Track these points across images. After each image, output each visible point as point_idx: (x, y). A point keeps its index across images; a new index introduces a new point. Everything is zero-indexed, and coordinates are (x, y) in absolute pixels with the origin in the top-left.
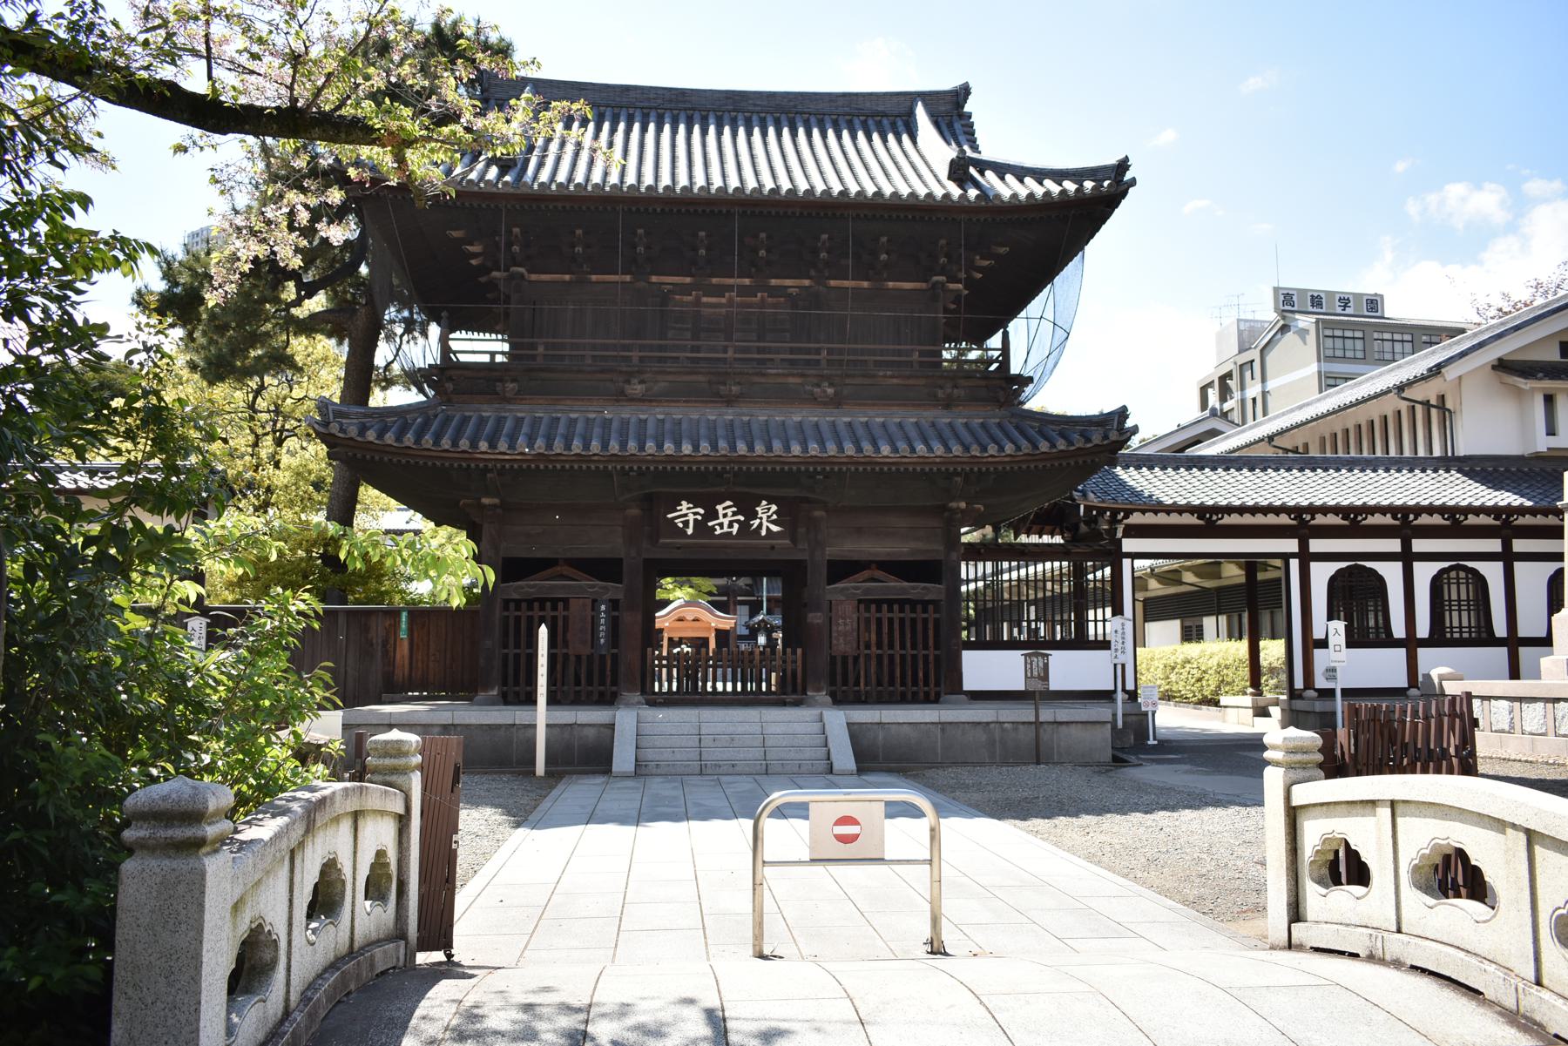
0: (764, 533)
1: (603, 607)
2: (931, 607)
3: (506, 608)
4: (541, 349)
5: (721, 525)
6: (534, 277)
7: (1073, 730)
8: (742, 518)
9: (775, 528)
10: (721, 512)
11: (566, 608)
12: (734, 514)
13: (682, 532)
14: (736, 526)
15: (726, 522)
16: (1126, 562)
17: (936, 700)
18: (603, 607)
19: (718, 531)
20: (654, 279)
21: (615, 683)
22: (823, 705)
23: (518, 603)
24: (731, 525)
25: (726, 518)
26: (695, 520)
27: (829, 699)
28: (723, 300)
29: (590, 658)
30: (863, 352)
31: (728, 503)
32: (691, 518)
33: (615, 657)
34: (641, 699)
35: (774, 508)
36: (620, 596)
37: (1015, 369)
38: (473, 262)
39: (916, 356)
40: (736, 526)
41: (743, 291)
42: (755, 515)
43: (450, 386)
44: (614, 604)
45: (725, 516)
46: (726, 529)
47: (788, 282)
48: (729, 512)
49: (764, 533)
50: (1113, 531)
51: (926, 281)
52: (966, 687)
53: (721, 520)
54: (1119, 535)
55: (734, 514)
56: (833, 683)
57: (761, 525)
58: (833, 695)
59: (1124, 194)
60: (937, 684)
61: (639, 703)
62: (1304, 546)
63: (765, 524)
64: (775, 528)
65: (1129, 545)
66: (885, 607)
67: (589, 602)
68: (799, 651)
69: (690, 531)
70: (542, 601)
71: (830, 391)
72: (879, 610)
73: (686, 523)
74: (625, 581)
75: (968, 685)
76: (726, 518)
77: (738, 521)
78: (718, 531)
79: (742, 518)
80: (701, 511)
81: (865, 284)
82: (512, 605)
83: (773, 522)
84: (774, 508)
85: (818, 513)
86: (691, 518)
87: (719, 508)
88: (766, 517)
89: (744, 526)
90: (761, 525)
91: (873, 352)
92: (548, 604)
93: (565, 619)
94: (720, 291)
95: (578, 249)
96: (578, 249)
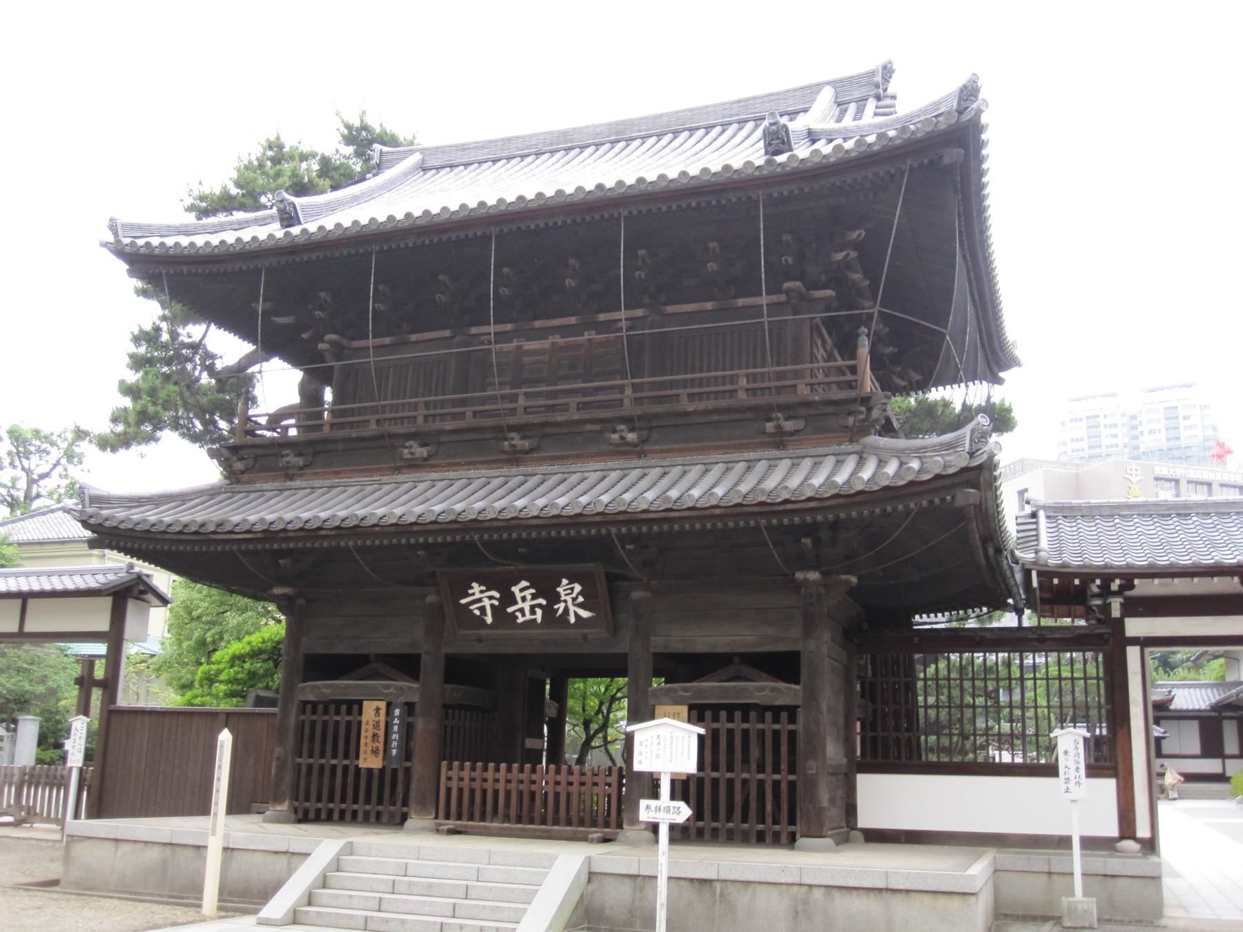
0: (572, 620)
1: (397, 712)
2: (784, 715)
5: (522, 611)
8: (544, 602)
9: (585, 614)
10: (518, 596)
11: (360, 713)
12: (534, 597)
13: (480, 621)
14: (539, 612)
15: (526, 606)
16: (1133, 653)
17: (791, 842)
18: (397, 712)
19: (520, 620)
21: (405, 803)
23: (314, 705)
24: (533, 612)
26: (492, 606)
29: (382, 771)
30: (673, 385)
31: (524, 584)
32: (487, 603)
33: (408, 771)
35: (578, 588)
36: (415, 698)
38: (304, 336)
39: (743, 382)
41: (564, 331)
42: (556, 598)
43: (239, 466)
44: (410, 708)
45: (524, 599)
46: (528, 617)
48: (528, 593)
49: (572, 620)
50: (1106, 608)
53: (520, 605)
54: (1116, 612)
55: (534, 597)
57: (566, 610)
60: (792, 821)
63: (572, 609)
64: (585, 614)
65: (1136, 627)
66: (723, 714)
67: (382, 705)
69: (489, 619)
70: (338, 703)
71: (631, 437)
72: (776, 720)
73: (483, 609)
75: (866, 819)
76: (526, 603)
77: (540, 606)
78: (520, 620)
79: (544, 602)
80: (497, 595)
83: (580, 605)
84: (578, 588)
85: (636, 595)
87: (515, 589)
89: (548, 611)
90: (566, 610)
91: (685, 383)
92: (344, 707)
93: (360, 723)
94: (544, 333)
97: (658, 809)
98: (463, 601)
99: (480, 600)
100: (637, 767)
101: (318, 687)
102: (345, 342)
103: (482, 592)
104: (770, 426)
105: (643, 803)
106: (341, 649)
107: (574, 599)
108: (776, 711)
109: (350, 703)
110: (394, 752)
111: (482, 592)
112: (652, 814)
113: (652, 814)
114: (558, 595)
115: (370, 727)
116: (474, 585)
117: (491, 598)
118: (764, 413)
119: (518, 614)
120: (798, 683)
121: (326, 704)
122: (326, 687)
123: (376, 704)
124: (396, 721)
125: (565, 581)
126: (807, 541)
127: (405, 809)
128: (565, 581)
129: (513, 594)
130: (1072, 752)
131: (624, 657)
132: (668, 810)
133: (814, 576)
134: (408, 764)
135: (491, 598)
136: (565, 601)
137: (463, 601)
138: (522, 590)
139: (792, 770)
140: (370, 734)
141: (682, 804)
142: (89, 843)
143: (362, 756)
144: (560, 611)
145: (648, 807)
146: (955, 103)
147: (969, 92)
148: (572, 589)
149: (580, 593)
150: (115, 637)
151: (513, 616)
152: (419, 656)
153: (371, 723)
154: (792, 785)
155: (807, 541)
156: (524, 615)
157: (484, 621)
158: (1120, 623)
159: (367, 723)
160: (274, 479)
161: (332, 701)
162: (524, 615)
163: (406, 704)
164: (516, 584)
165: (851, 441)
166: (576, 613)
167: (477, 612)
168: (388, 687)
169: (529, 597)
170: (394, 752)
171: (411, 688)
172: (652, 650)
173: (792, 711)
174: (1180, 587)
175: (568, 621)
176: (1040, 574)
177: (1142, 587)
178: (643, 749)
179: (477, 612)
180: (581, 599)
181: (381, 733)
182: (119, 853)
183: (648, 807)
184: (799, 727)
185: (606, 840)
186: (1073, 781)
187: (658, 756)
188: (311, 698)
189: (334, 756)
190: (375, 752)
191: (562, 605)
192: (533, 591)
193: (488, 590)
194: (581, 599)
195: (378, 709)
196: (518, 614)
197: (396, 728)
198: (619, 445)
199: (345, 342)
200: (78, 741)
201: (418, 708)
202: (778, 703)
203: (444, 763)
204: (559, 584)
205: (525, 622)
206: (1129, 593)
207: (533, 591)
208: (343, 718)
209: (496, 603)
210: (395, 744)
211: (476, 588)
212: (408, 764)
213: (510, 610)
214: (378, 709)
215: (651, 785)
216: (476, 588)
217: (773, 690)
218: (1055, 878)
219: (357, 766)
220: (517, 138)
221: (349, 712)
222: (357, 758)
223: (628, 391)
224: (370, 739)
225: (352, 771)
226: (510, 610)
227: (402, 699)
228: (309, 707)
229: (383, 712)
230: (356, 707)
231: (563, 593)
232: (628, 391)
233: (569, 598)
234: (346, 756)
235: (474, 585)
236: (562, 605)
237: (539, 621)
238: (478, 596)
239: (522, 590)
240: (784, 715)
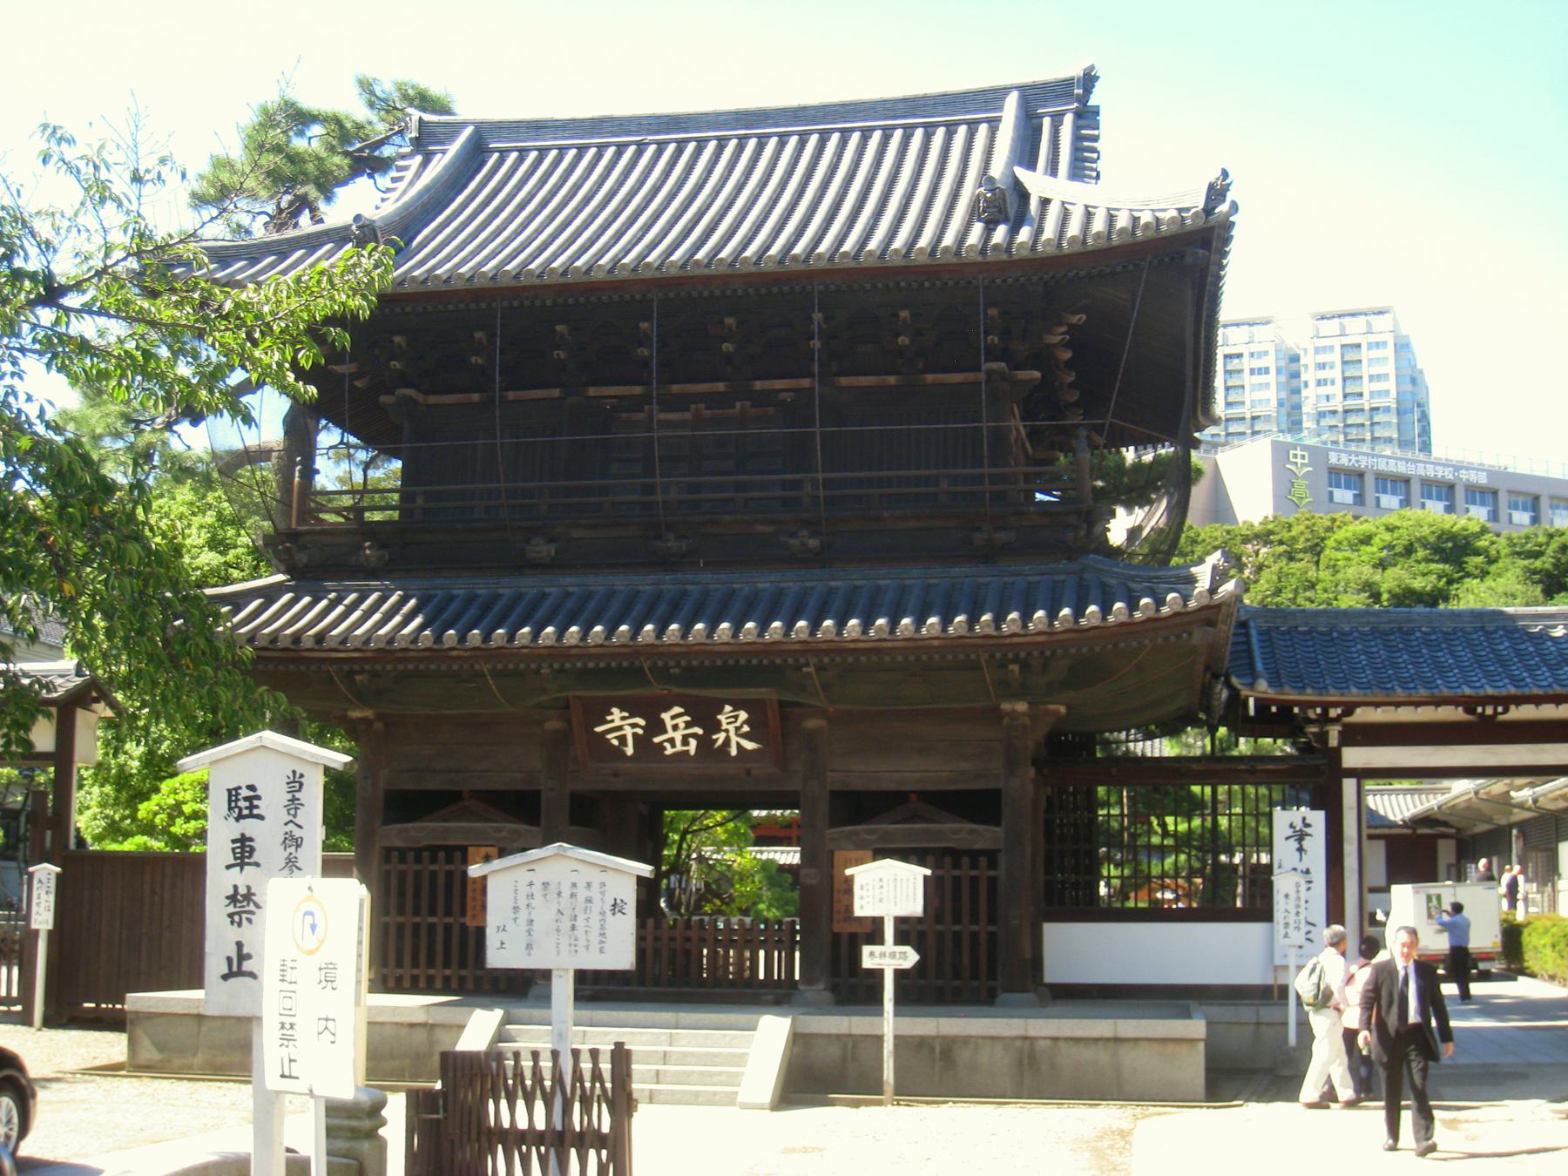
0: (734, 752)
2: (983, 861)
5: (672, 741)
6: (433, 399)
8: (700, 731)
9: (749, 745)
10: (669, 723)
13: (618, 752)
14: (693, 743)
15: (678, 736)
16: (1349, 785)
19: (669, 751)
20: (592, 391)
23: (402, 853)
24: (685, 742)
26: (635, 735)
27: (827, 995)
28: (687, 416)
31: (677, 710)
32: (628, 731)
35: (743, 715)
39: (944, 485)
41: (712, 400)
42: (717, 727)
45: (675, 727)
46: (679, 747)
47: (779, 384)
48: (681, 721)
49: (734, 752)
50: (1323, 737)
53: (671, 734)
54: (1333, 742)
55: (688, 725)
57: (727, 740)
58: (834, 989)
59: (1227, 226)
60: (992, 975)
63: (734, 739)
64: (749, 745)
65: (1353, 757)
69: (630, 751)
71: (813, 543)
72: (956, 865)
73: (623, 739)
74: (543, 823)
77: (694, 735)
78: (669, 751)
79: (700, 731)
80: (642, 722)
81: (892, 380)
83: (745, 736)
84: (743, 715)
85: (812, 723)
86: (628, 731)
87: (666, 716)
89: (705, 743)
90: (727, 740)
92: (442, 855)
95: (903, 340)
96: (903, 340)
97: (883, 955)
98: (599, 729)
99: (620, 728)
102: (420, 397)
103: (623, 718)
105: (866, 950)
106: (432, 784)
107: (737, 729)
108: (974, 855)
109: (450, 851)
111: (623, 718)
112: (877, 961)
113: (877, 961)
114: (719, 723)
116: (615, 710)
117: (634, 726)
120: (998, 824)
121: (418, 852)
125: (728, 708)
126: (1015, 668)
128: (728, 708)
129: (662, 722)
131: (796, 793)
132: (893, 955)
133: (1022, 707)
135: (634, 726)
136: (727, 731)
137: (599, 729)
138: (673, 718)
139: (992, 920)
141: (908, 949)
143: (469, 913)
144: (720, 742)
145: (872, 954)
148: (736, 717)
149: (745, 722)
151: (661, 747)
152: (538, 792)
154: (992, 937)
155: (1015, 668)
156: (673, 746)
157: (624, 753)
158: (1336, 754)
161: (429, 848)
162: (673, 746)
164: (666, 709)
166: (738, 744)
167: (615, 742)
168: (499, 830)
169: (682, 725)
173: (992, 856)
175: (728, 753)
178: (864, 893)
179: (615, 742)
180: (746, 728)
183: (872, 954)
184: (1001, 873)
188: (399, 843)
189: (433, 913)
191: (721, 737)
192: (687, 718)
193: (631, 716)
194: (746, 728)
199: (420, 397)
200: (44, 896)
202: (977, 846)
204: (720, 711)
205: (674, 754)
206: (1347, 720)
207: (687, 718)
208: (441, 867)
209: (640, 731)
211: (616, 714)
213: (657, 740)
215: (872, 931)
216: (616, 714)
217: (971, 832)
218: (1264, 1028)
219: (464, 928)
221: (449, 861)
222: (463, 913)
225: (456, 930)
226: (657, 740)
228: (395, 854)
230: (458, 855)
231: (724, 722)
233: (731, 728)
234: (448, 913)
235: (615, 710)
236: (721, 737)
237: (692, 752)
238: (618, 723)
239: (673, 718)
240: (983, 861)
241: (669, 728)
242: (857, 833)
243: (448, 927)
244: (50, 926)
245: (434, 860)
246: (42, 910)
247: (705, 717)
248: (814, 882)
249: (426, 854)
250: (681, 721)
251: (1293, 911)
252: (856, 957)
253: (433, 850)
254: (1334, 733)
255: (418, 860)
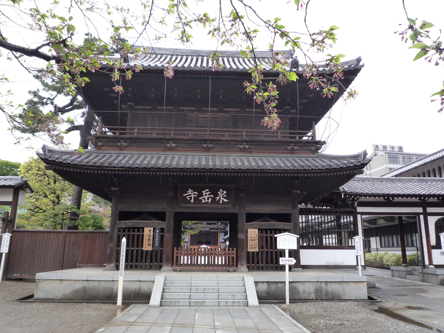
0: (221, 202)
1: (157, 231)
3: (119, 231)
4: (136, 130)
5: (204, 199)
7: (351, 285)
8: (212, 196)
9: (225, 200)
10: (204, 194)
11: (143, 231)
12: (210, 194)
13: (189, 202)
14: (210, 199)
15: (206, 198)
16: (359, 216)
18: (157, 231)
21: (161, 262)
22: (244, 272)
24: (208, 199)
25: (206, 196)
27: (247, 269)
29: (152, 251)
31: (207, 190)
32: (193, 196)
33: (162, 251)
34: (171, 268)
35: (225, 192)
37: (318, 139)
40: (210, 199)
42: (217, 195)
43: (100, 144)
44: (162, 230)
45: (206, 195)
46: (206, 201)
47: (231, 109)
48: (207, 193)
49: (221, 202)
51: (282, 109)
52: (301, 264)
53: (204, 197)
54: (356, 205)
55: (210, 194)
56: (248, 262)
57: (220, 199)
58: (248, 267)
61: (170, 270)
62: (425, 210)
63: (222, 198)
64: (225, 200)
65: (359, 209)
66: (269, 232)
67: (152, 229)
68: (235, 249)
69: (192, 201)
71: (247, 147)
72: (266, 233)
73: (191, 198)
74: (167, 220)
76: (206, 196)
77: (211, 197)
79: (212, 196)
80: (197, 193)
82: (122, 230)
83: (224, 198)
84: (225, 192)
86: (193, 196)
87: (204, 192)
88: (222, 196)
89: (213, 199)
93: (143, 235)
98: (184, 195)
99: (190, 195)
100: (278, 248)
101: (126, 223)
103: (192, 192)
104: (289, 148)
105: (281, 259)
107: (223, 196)
109: (139, 229)
110: (157, 244)
111: (192, 192)
112: (284, 262)
113: (284, 262)
115: (147, 236)
116: (190, 190)
117: (194, 194)
118: (288, 143)
119: (203, 200)
120: (290, 223)
122: (129, 223)
123: (149, 228)
124: (157, 234)
125: (221, 190)
127: (160, 264)
128: (221, 190)
130: (359, 242)
132: (289, 261)
134: (161, 249)
135: (194, 194)
136: (220, 196)
137: (184, 195)
138: (206, 192)
140: (147, 239)
141: (293, 259)
142: (47, 282)
143: (144, 246)
146: (355, 63)
147: (359, 60)
148: (223, 193)
150: (14, 204)
151: (201, 200)
152: (165, 213)
153: (147, 235)
156: (205, 200)
158: (355, 209)
159: (146, 235)
160: (115, 150)
161: (132, 228)
162: (205, 200)
163: (161, 228)
165: (313, 154)
167: (189, 199)
168: (154, 223)
169: (208, 194)
170: (157, 244)
171: (163, 223)
172: (246, 212)
174: (372, 199)
176: (344, 194)
177: (363, 199)
178: (280, 242)
179: (189, 199)
180: (225, 196)
181: (152, 238)
182: (63, 285)
183: (282, 260)
185: (234, 271)
186: (359, 250)
187: (285, 244)
189: (133, 247)
190: (149, 245)
191: (219, 197)
194: (225, 196)
195: (150, 230)
196: (203, 200)
197: (157, 237)
198: (243, 149)
200: (6, 243)
201: (165, 230)
203: (175, 248)
208: (136, 233)
209: (196, 196)
210: (157, 242)
212: (161, 249)
213: (200, 198)
214: (150, 230)
215: (282, 253)
219: (142, 250)
220: (179, 49)
221: (138, 231)
222: (142, 247)
223: (244, 133)
224: (147, 241)
225: (140, 251)
226: (200, 198)
227: (159, 227)
229: (152, 231)
230: (141, 230)
232: (244, 133)
233: (221, 195)
234: (137, 246)
235: (190, 190)
236: (219, 197)
238: (190, 193)
239: (206, 192)
241: (204, 195)
242: (254, 224)
243: (137, 250)
244: (7, 252)
245: (134, 231)
246: (4, 246)
247: (214, 193)
248: (243, 237)
249: (132, 230)
250: (207, 193)
251: (359, 246)
252: (277, 261)
253: (134, 229)
254: (356, 203)
255: (129, 231)
